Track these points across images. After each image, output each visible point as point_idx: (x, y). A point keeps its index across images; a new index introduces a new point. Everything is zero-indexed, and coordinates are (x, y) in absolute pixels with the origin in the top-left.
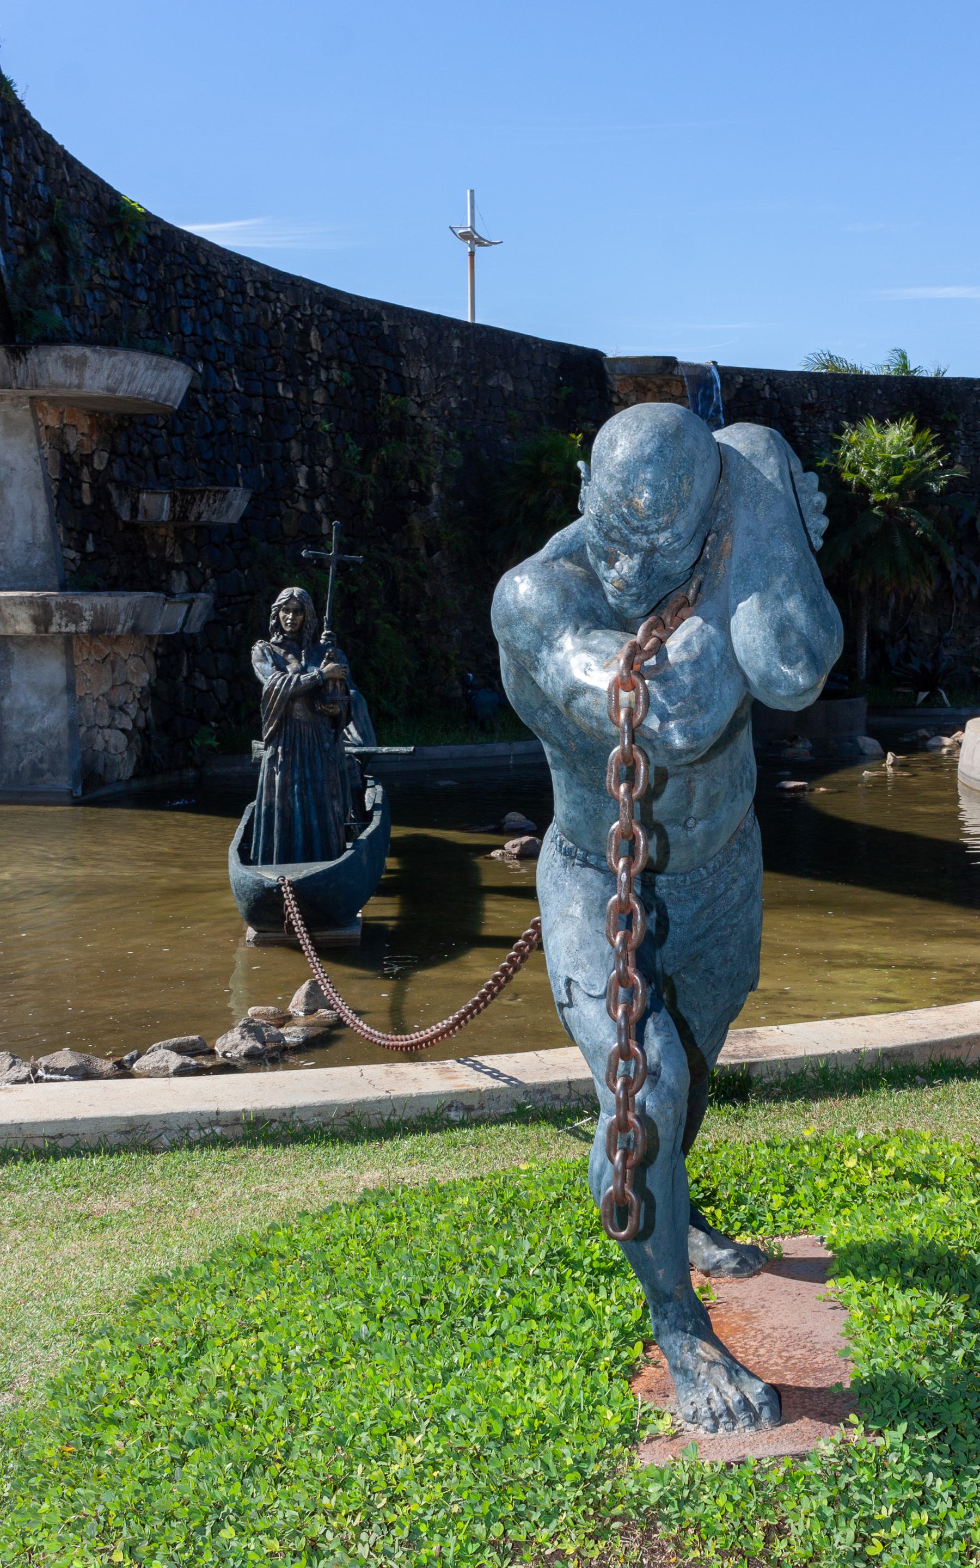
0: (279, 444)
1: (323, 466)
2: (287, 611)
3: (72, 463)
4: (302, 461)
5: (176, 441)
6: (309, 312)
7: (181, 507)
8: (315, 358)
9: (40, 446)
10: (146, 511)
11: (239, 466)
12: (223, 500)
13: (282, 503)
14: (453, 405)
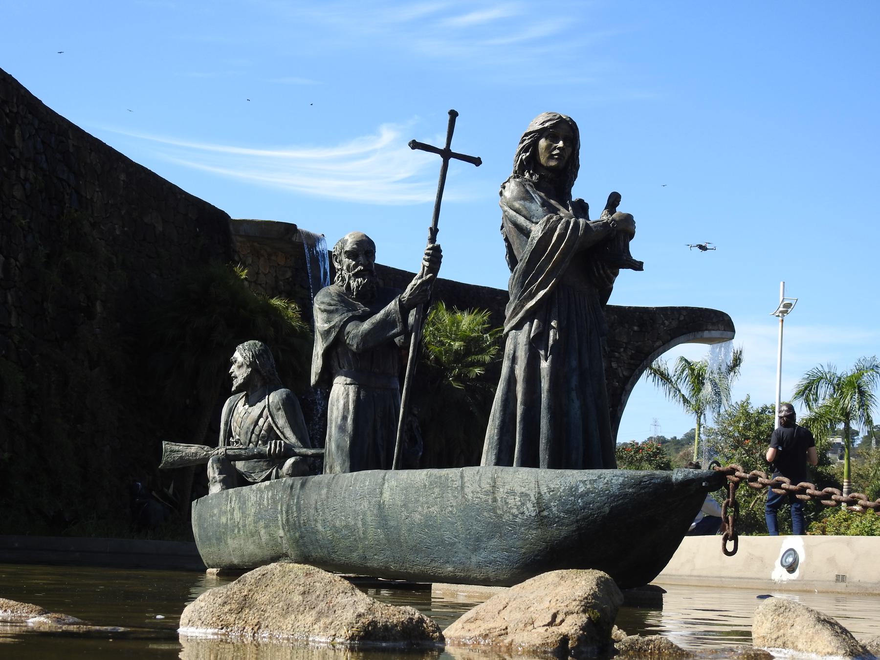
1: (16, 260)
6: (15, 110)
8: (17, 155)
14: (118, 232)
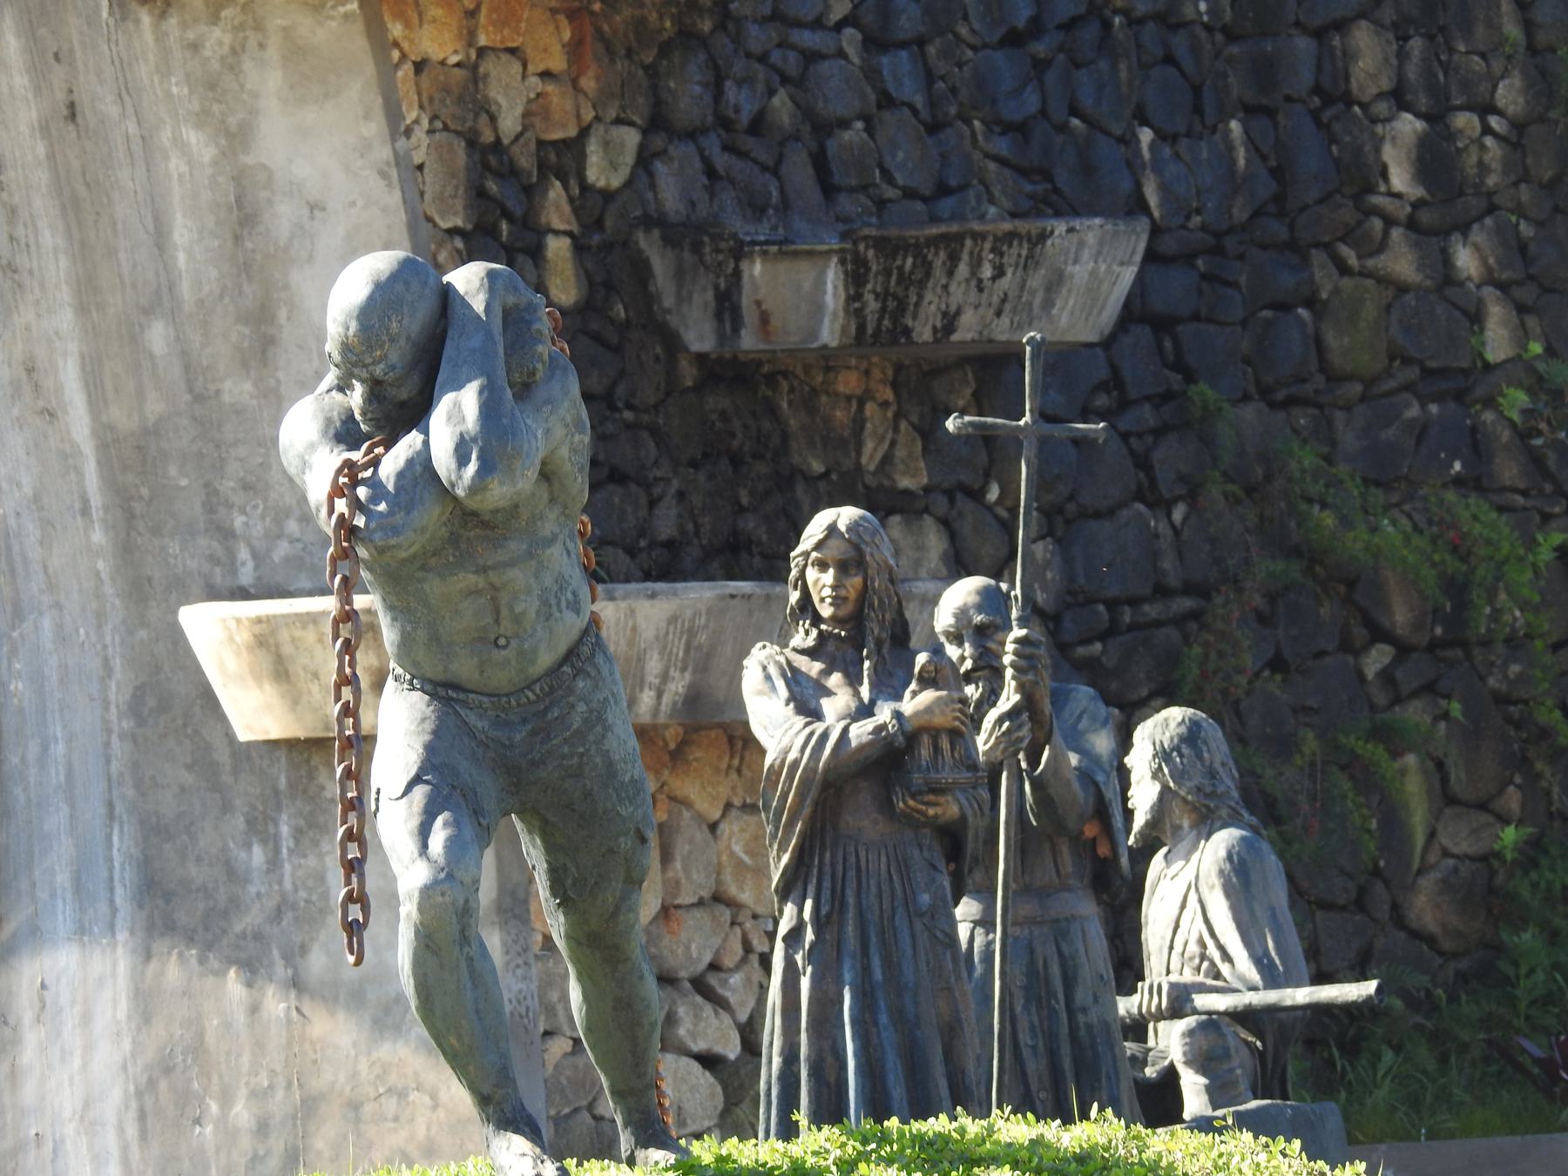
0: (1303, 44)
1: (1486, 109)
2: (822, 566)
3: (510, 172)
4: (1399, 98)
5: (899, 69)
7: (883, 296)
9: (398, 128)
10: (765, 319)
11: (1146, 135)
12: (1030, 263)
13: (1318, 257)
